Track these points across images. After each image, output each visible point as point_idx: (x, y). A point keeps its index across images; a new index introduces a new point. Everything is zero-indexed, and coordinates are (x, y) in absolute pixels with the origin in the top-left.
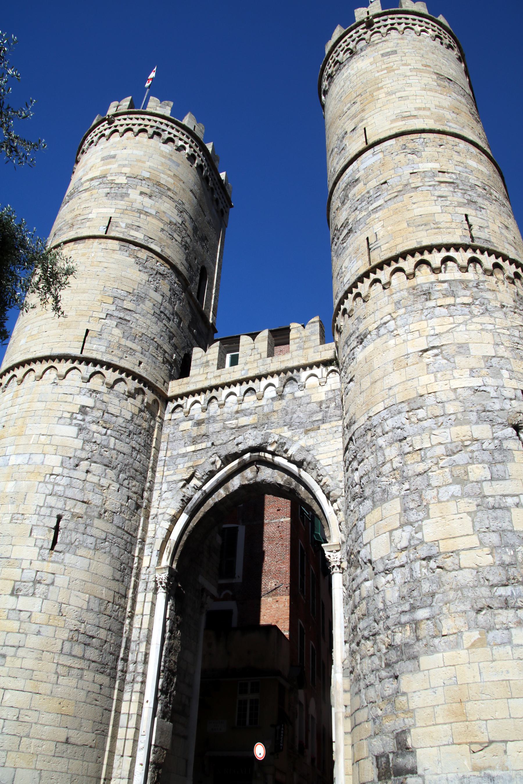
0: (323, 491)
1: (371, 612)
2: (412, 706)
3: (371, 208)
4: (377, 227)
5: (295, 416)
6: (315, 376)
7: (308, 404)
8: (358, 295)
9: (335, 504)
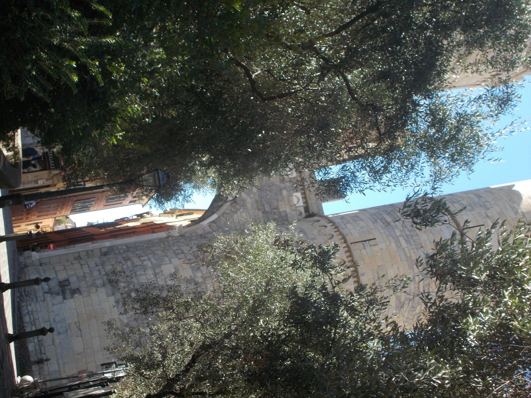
0: (216, 219)
1: (135, 268)
2: (92, 295)
3: (401, 239)
4: (383, 246)
5: (268, 192)
6: (298, 202)
7: (277, 200)
8: (333, 236)
9: (208, 227)
